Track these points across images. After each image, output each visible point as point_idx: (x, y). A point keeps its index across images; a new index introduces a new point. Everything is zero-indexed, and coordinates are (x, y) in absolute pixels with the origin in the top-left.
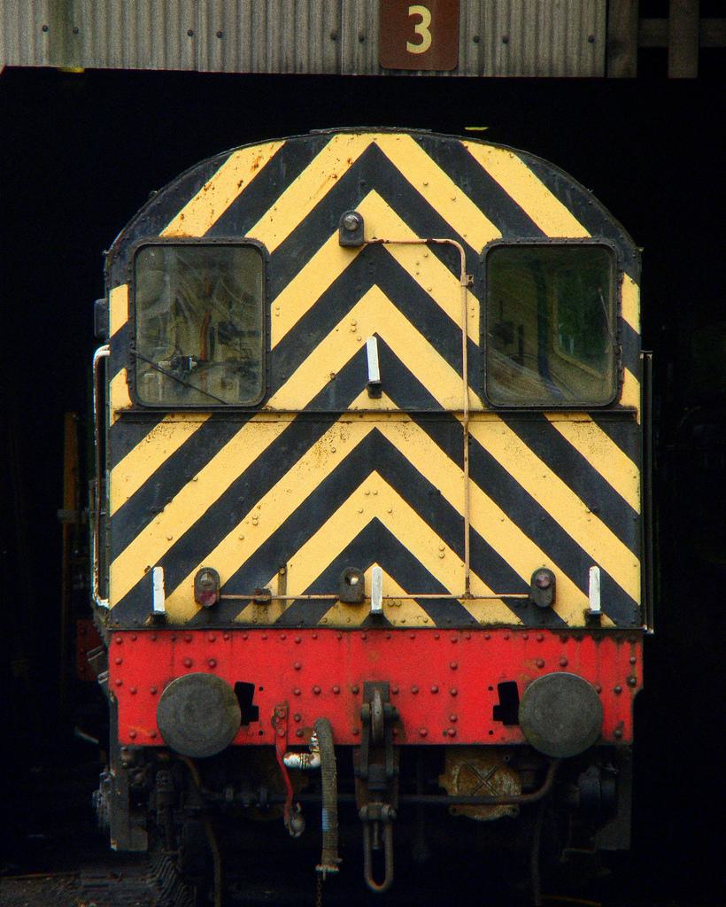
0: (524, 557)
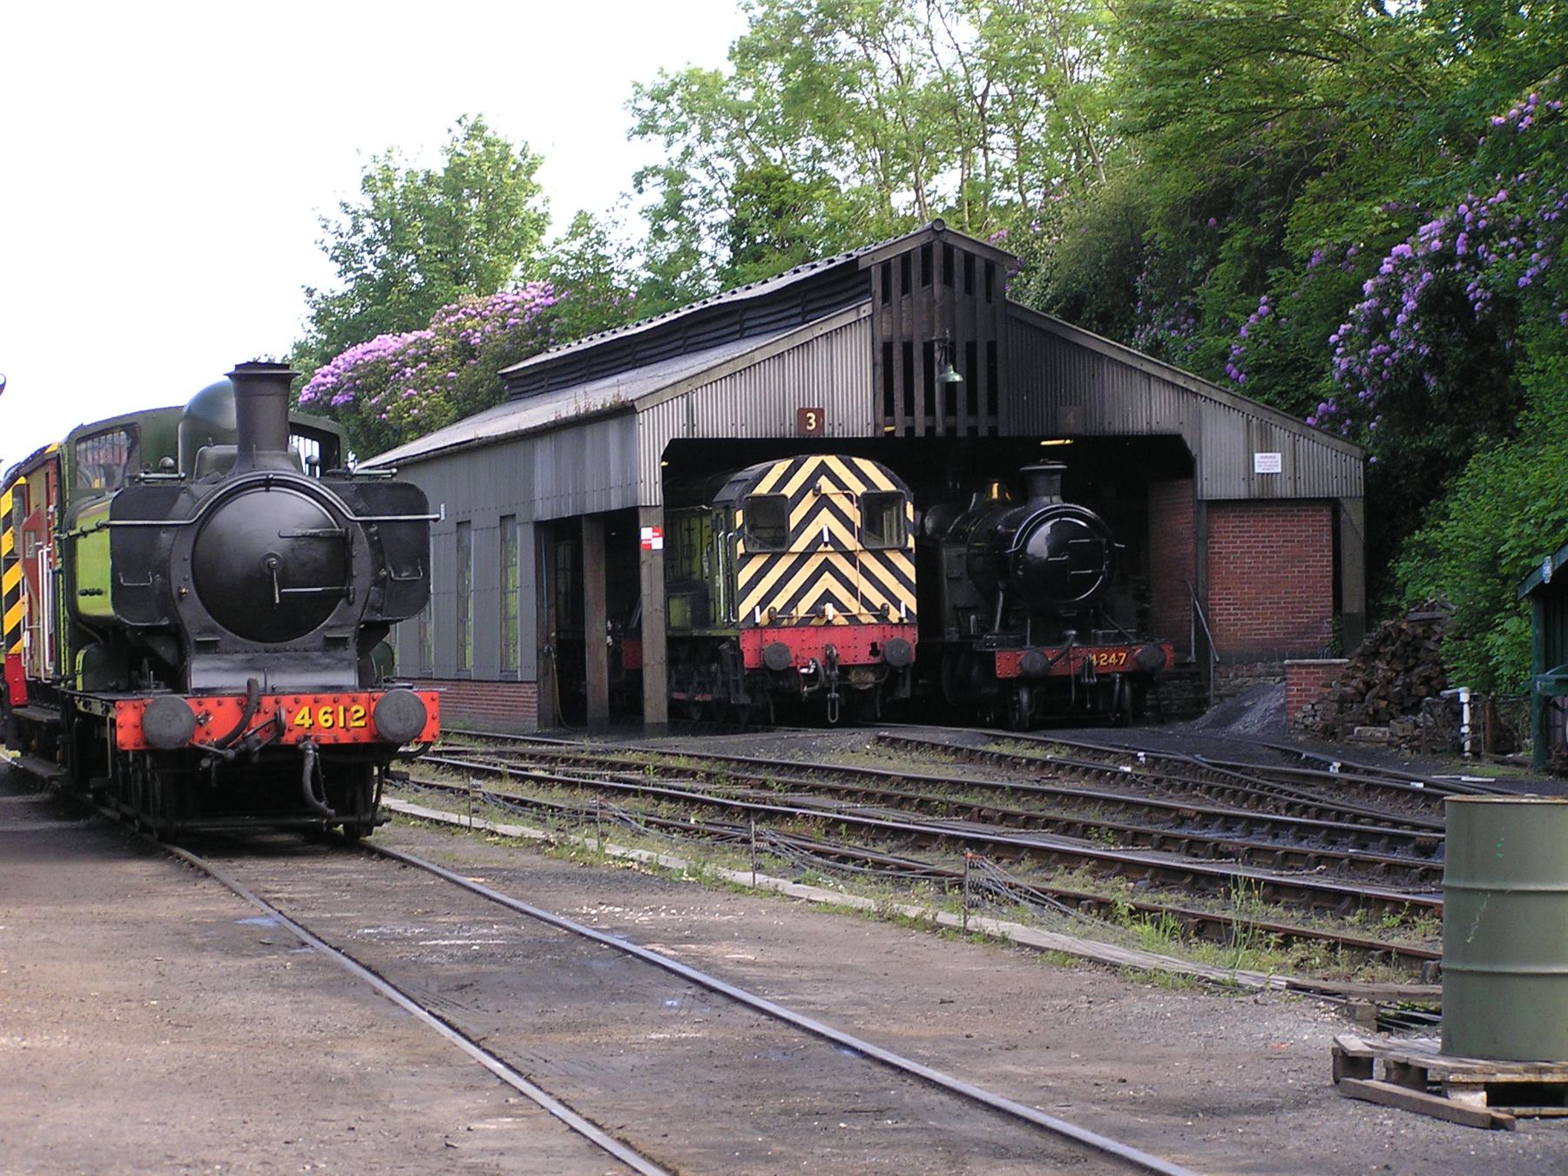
0: (878, 600)
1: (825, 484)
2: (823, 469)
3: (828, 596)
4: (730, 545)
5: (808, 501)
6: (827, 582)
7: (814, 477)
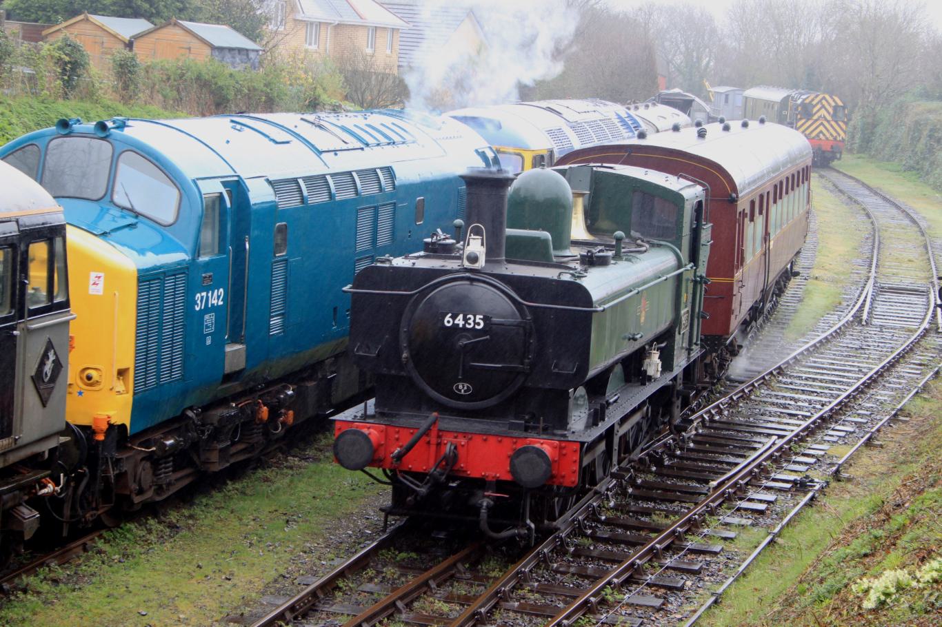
0: (835, 134)
1: (824, 102)
2: (824, 98)
3: (821, 132)
4: (797, 115)
5: (819, 106)
6: (821, 128)
7: (820, 101)
